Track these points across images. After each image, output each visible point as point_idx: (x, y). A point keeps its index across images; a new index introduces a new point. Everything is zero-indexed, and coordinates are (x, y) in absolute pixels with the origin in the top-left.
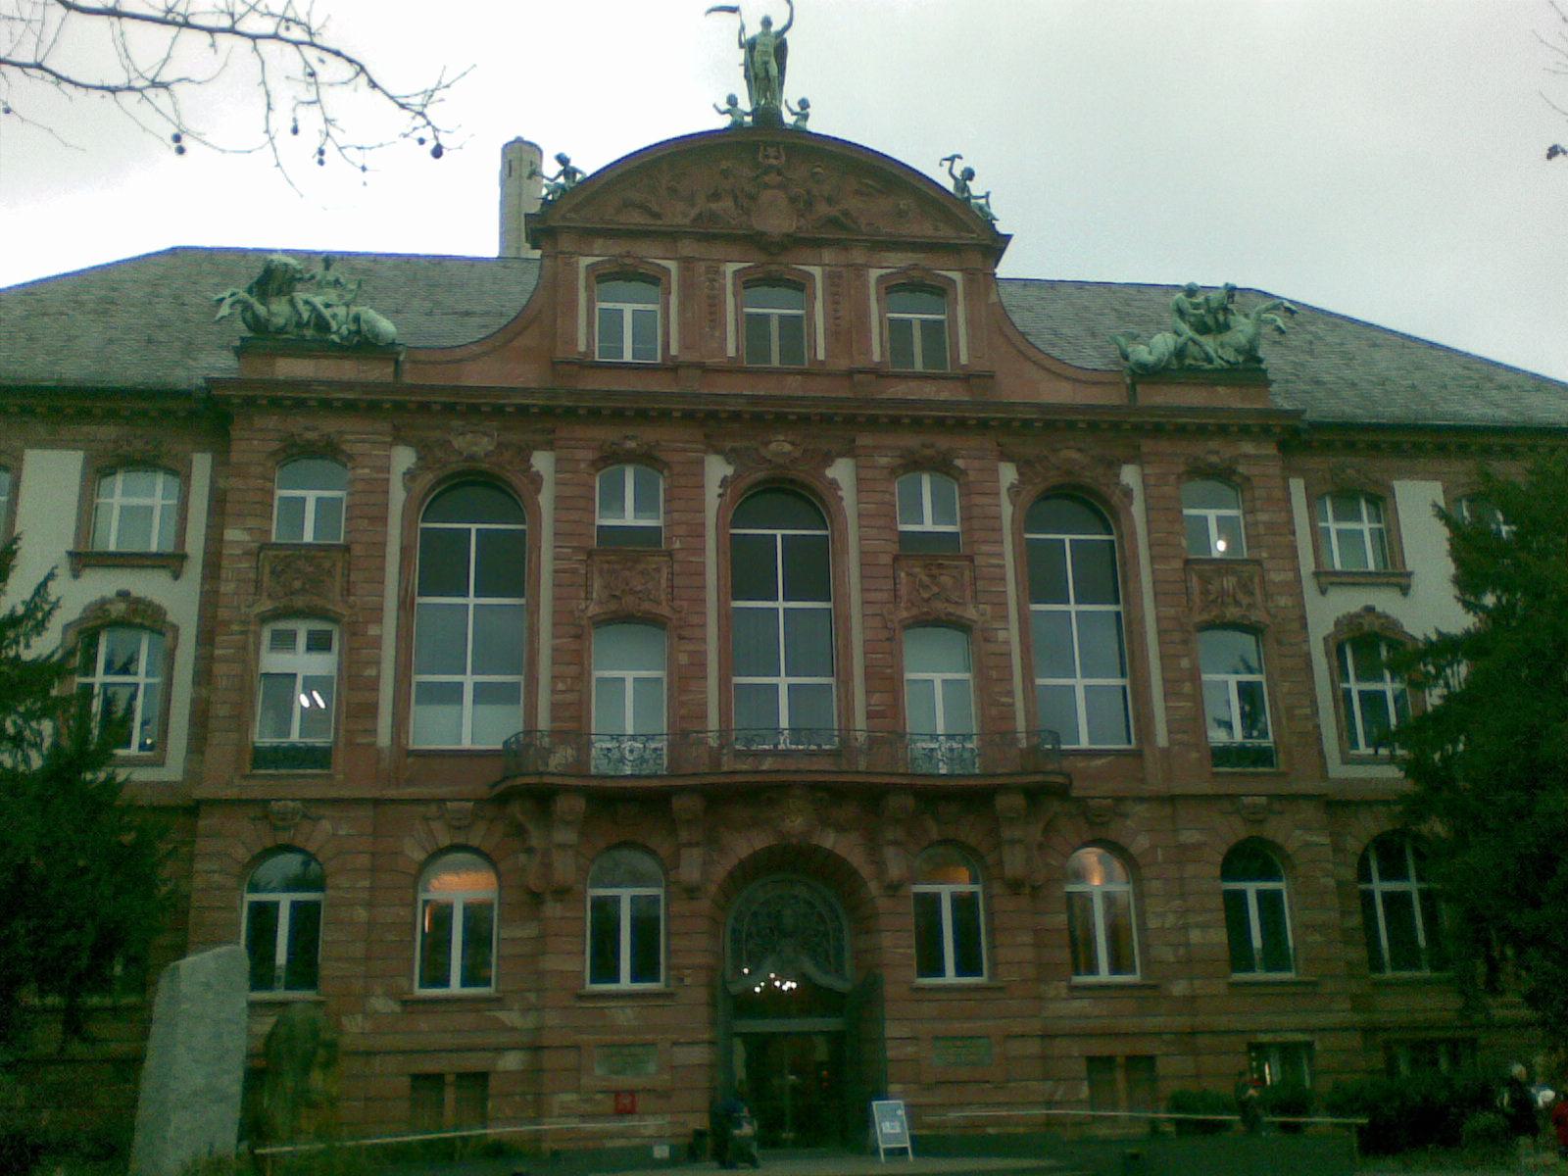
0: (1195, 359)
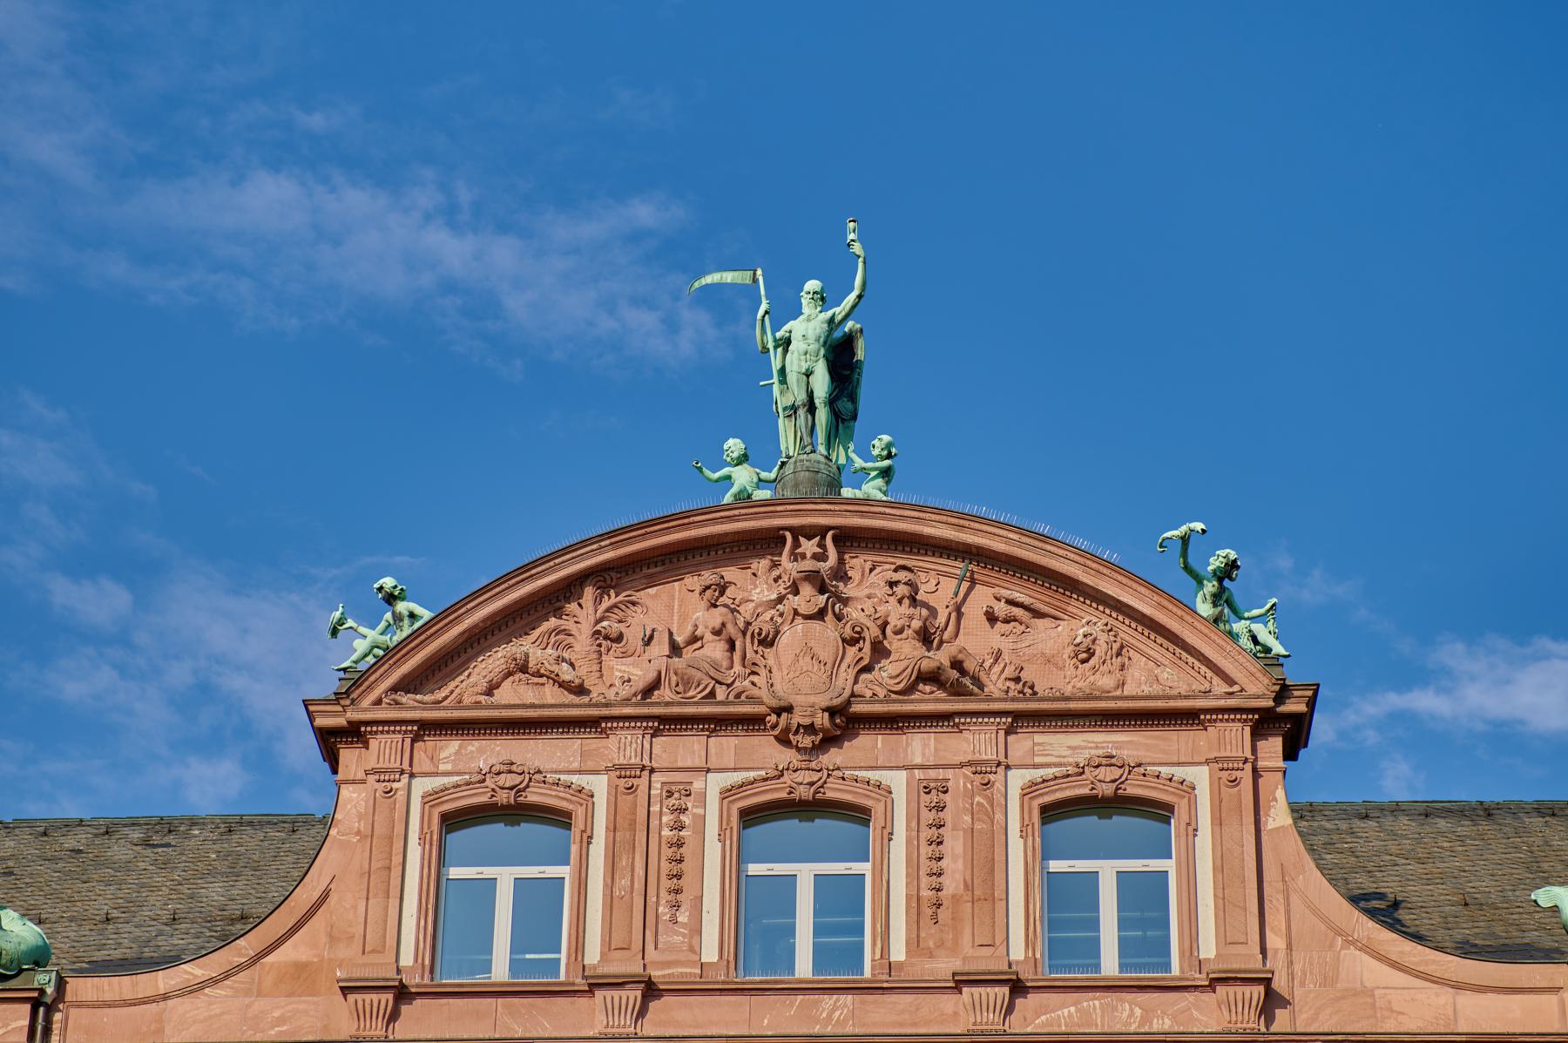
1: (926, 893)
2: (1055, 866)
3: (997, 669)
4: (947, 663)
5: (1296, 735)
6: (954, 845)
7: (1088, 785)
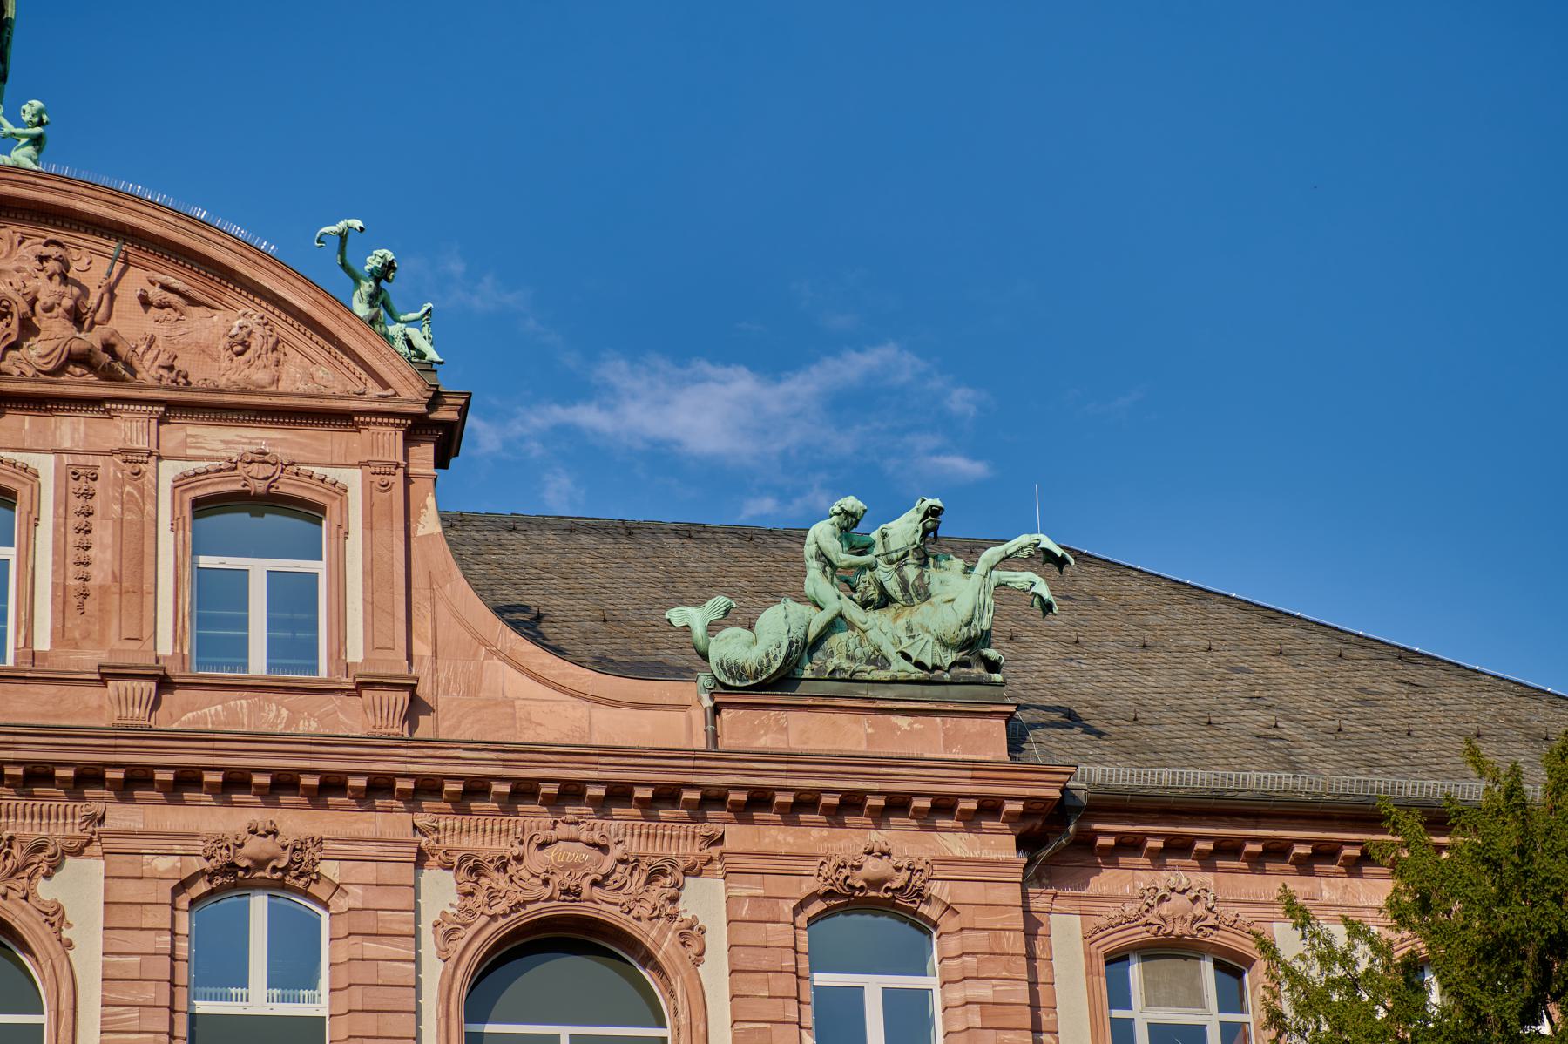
0: (850, 658)
1: (72, 582)
2: (206, 561)
3: (150, 355)
4: (98, 346)
5: (447, 440)
6: (103, 534)
7: (240, 480)
